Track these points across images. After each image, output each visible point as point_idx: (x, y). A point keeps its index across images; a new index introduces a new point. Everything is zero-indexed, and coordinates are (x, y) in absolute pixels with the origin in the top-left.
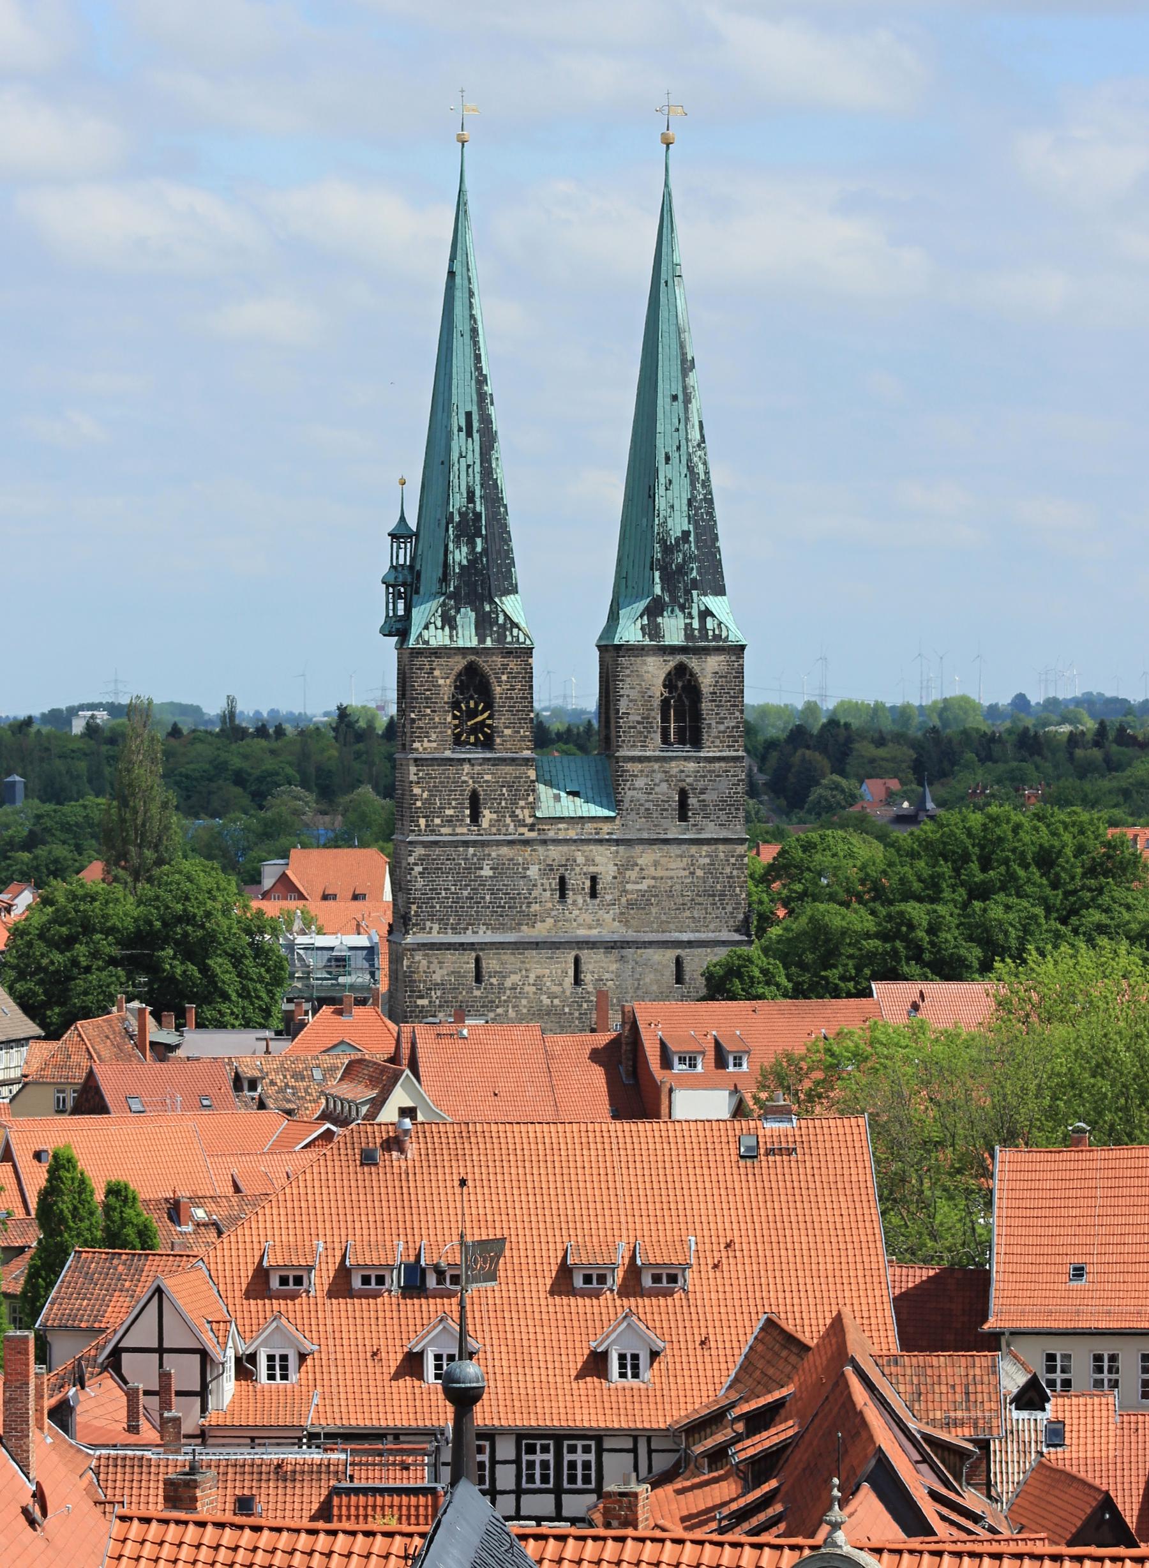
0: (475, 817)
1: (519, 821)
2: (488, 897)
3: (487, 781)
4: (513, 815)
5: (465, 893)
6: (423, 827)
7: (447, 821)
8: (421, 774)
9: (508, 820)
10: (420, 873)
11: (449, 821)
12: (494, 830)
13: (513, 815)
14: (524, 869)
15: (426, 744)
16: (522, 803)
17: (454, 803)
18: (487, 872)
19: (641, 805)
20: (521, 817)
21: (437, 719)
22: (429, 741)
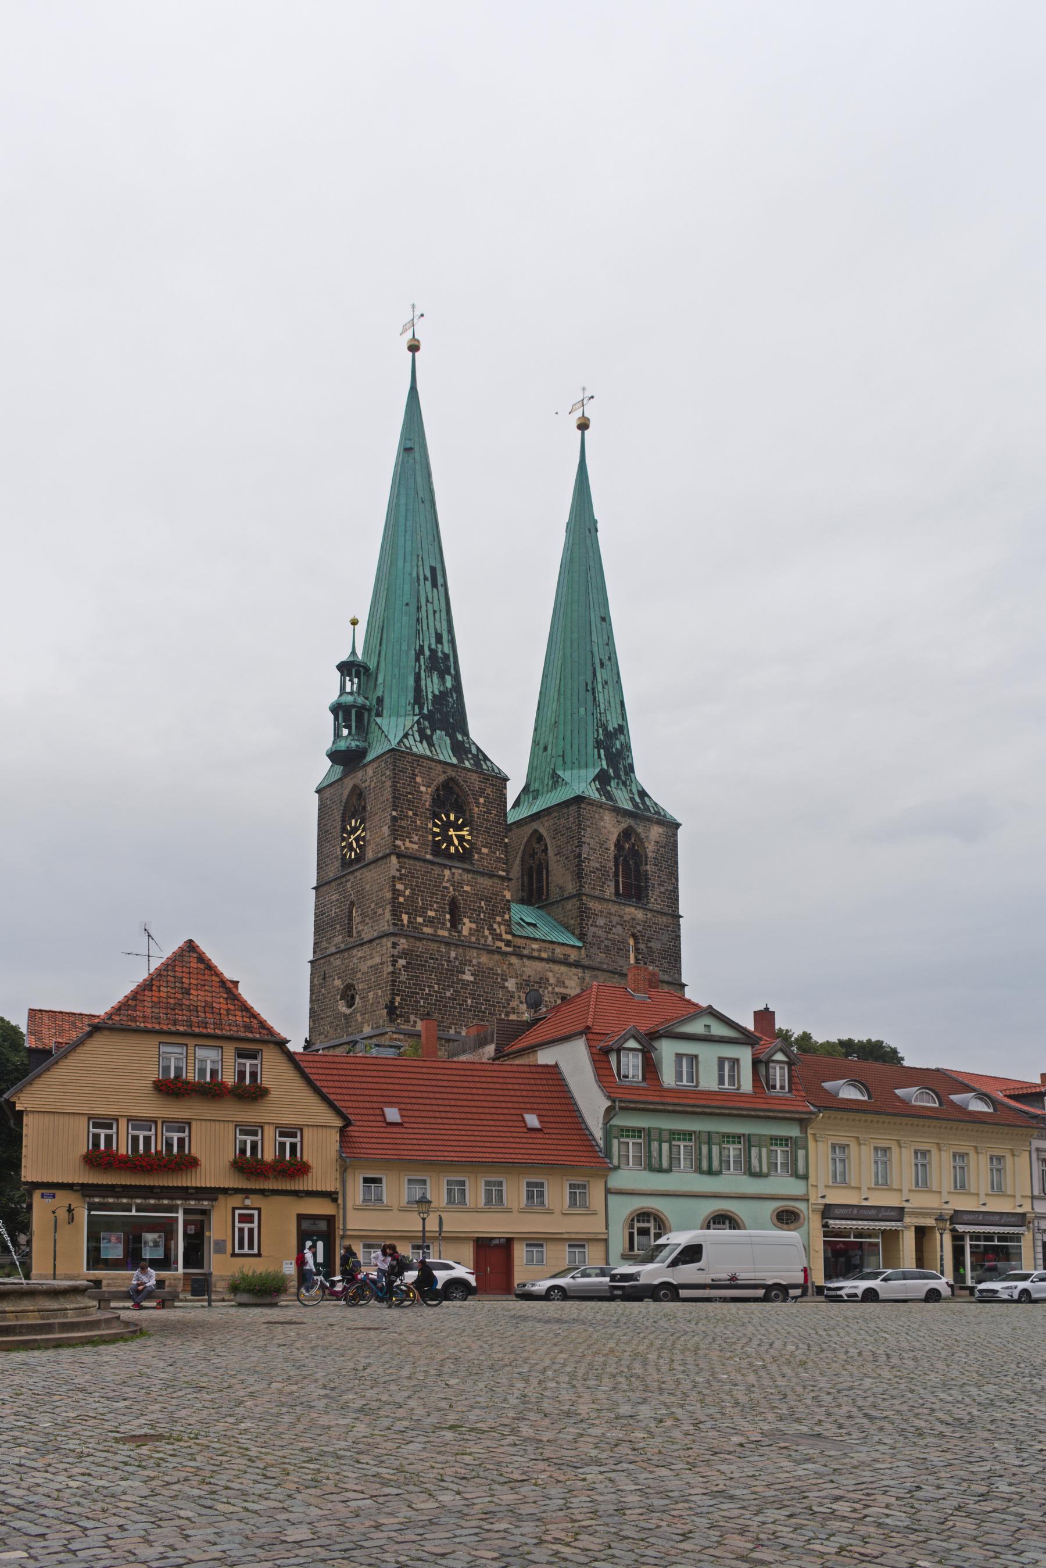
0: (455, 922)
1: (497, 935)
2: (469, 1001)
4: (491, 929)
5: (448, 994)
6: (405, 922)
7: (429, 921)
8: (403, 871)
9: (487, 932)
10: (403, 966)
11: (430, 921)
12: (473, 939)
13: (491, 929)
14: (502, 979)
15: (408, 844)
16: (499, 919)
19: (602, 941)
21: (419, 823)
22: (411, 842)
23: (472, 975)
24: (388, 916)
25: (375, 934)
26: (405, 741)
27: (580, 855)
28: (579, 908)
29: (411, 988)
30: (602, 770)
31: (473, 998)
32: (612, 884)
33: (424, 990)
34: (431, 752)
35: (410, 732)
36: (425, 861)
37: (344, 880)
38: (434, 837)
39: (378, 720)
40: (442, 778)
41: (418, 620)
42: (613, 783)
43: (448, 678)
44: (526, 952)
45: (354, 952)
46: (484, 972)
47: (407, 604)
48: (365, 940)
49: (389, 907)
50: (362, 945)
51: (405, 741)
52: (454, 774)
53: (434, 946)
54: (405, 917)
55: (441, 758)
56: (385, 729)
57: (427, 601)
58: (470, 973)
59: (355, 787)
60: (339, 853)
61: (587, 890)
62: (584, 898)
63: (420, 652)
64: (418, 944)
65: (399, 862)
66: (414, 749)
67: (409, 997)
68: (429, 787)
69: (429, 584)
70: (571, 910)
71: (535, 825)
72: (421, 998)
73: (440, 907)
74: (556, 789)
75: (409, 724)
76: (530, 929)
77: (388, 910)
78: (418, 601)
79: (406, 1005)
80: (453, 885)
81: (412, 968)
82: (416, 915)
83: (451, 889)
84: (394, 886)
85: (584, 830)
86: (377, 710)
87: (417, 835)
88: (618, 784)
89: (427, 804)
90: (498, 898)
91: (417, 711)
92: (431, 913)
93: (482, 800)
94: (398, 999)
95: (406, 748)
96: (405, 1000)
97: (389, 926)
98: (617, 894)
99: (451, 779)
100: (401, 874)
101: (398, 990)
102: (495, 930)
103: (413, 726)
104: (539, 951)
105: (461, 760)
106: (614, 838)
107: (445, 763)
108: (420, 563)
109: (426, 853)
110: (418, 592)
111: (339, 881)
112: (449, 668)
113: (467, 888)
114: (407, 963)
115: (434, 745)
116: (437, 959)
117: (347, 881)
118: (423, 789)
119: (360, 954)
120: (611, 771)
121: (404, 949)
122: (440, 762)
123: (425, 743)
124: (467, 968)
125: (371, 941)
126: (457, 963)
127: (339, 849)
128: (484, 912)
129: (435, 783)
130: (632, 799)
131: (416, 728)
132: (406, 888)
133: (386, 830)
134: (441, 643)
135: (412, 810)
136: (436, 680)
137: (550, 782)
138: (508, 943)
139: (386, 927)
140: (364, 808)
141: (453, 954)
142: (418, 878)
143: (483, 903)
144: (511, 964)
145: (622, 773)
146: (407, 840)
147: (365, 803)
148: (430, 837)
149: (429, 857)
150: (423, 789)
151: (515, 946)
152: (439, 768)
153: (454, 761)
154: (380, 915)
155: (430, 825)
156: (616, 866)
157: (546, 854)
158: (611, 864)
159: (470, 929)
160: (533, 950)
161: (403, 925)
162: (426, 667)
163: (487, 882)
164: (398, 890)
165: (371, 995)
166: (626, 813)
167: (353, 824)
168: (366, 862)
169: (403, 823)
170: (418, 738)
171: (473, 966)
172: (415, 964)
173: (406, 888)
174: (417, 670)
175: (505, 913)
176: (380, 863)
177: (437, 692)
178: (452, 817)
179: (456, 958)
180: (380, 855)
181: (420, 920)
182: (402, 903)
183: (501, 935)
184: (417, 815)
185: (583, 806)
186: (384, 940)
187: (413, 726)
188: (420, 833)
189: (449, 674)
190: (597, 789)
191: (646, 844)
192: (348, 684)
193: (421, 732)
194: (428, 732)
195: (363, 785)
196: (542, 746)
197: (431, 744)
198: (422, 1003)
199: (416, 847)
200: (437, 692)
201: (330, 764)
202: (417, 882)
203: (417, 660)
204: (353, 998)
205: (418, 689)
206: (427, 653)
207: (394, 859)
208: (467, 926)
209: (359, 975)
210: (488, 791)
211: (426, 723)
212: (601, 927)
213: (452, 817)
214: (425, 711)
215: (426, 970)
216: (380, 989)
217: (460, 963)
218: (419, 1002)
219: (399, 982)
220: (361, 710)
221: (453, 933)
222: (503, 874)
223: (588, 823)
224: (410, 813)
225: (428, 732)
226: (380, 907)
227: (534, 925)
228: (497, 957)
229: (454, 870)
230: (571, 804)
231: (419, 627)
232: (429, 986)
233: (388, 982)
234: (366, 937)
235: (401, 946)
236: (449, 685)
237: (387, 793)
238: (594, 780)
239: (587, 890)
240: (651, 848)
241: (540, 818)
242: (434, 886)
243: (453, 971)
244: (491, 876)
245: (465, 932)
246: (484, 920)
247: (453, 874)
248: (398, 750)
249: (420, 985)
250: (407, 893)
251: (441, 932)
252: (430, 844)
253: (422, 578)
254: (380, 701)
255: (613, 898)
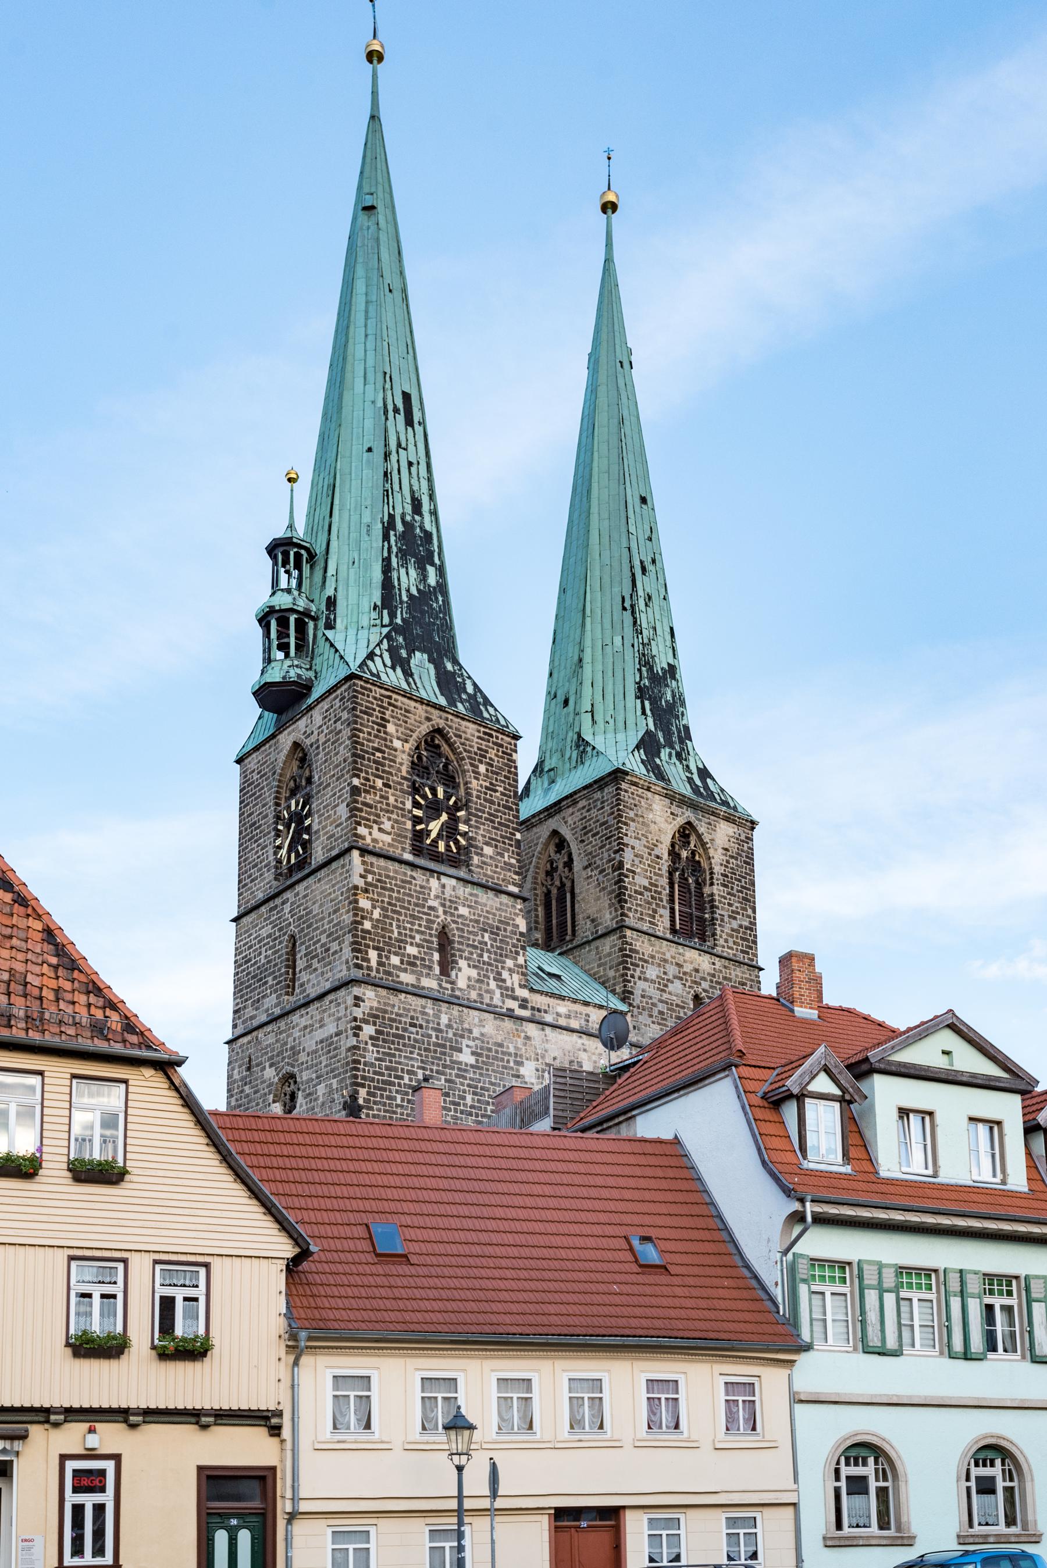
0: (447, 966)
1: (507, 989)
3: (459, 916)
4: (499, 978)
6: (374, 963)
7: (411, 964)
8: (370, 878)
9: (493, 984)
10: (371, 1038)
11: (411, 963)
13: (499, 978)
15: (376, 834)
16: (509, 963)
17: (418, 937)
18: (466, 1057)
20: (509, 984)
21: (392, 800)
22: (380, 830)
23: (473, 1053)
24: (347, 952)
25: (328, 986)
26: (369, 663)
27: (621, 865)
28: (621, 950)
29: (383, 1075)
30: (648, 732)
31: (475, 1093)
32: (666, 913)
33: (402, 1078)
34: (409, 684)
35: (377, 651)
36: (402, 862)
37: (278, 901)
38: (414, 826)
39: (329, 634)
40: (425, 728)
41: (386, 474)
42: (664, 753)
43: (431, 571)
44: (549, 1018)
45: (295, 1018)
46: (490, 1050)
47: (370, 450)
48: (313, 996)
49: (349, 939)
50: (306, 1004)
51: (369, 663)
52: (442, 723)
53: (416, 1003)
54: (373, 955)
55: (424, 695)
56: (339, 646)
57: (399, 445)
58: (469, 1050)
59: (296, 745)
60: (271, 858)
61: (630, 921)
62: (628, 933)
63: (389, 526)
64: (393, 999)
65: (364, 863)
66: (383, 677)
67: (380, 1089)
68: (406, 741)
69: (401, 418)
70: (610, 954)
71: (553, 824)
72: (397, 1092)
73: (425, 940)
74: (582, 763)
75: (375, 639)
76: (553, 982)
77: (347, 943)
78: (386, 445)
79: (375, 1103)
80: (443, 905)
81: (384, 1041)
82: (389, 952)
83: (441, 910)
84: (356, 901)
85: (626, 824)
86: (327, 618)
87: (389, 819)
88: (670, 755)
89: (404, 769)
90: (509, 928)
91: (386, 620)
92: (411, 950)
93: (482, 768)
94: (363, 1093)
95: (372, 674)
96: (374, 1095)
97: (348, 969)
98: (673, 931)
99: (439, 731)
100: (366, 883)
101: (364, 1078)
102: (504, 981)
103: (381, 642)
104: (568, 1017)
105: (452, 703)
106: (667, 840)
107: (429, 704)
108: (388, 386)
109: (403, 849)
110: (386, 431)
111: (271, 904)
112: (432, 553)
113: (463, 911)
114: (377, 1032)
115: (412, 675)
116: (421, 1027)
117: (283, 903)
118: (397, 744)
119: (304, 1022)
120: (660, 735)
121: (371, 1008)
122: (421, 701)
123: (399, 670)
124: (465, 1042)
125: (321, 997)
126: (450, 1035)
127: (271, 852)
128: (488, 951)
129: (415, 736)
130: (690, 780)
131: (385, 645)
132: (374, 907)
133: (343, 811)
134: (420, 514)
135: (382, 778)
136: (413, 573)
137: (575, 754)
138: (524, 1004)
139: (344, 972)
140: (309, 780)
141: (444, 1019)
142: (392, 890)
143: (486, 935)
144: (528, 1038)
145: (675, 739)
146: (375, 826)
147: (311, 771)
148: (409, 825)
149: (408, 856)
150: (397, 744)
151: (533, 1008)
152: (421, 710)
153: (442, 701)
154: (336, 952)
155: (409, 805)
156: (671, 884)
157: (571, 870)
158: (664, 881)
159: (469, 979)
160: (558, 1014)
161: (369, 968)
162: (400, 550)
163: (488, 899)
164: (363, 910)
165: (321, 1089)
166: (683, 801)
167: (293, 808)
168: (313, 866)
169: (369, 799)
170: (389, 663)
171: (474, 1039)
172: (388, 1034)
173: (374, 907)
174: (386, 554)
175: (517, 953)
176: (334, 865)
177: (414, 591)
178: (440, 792)
179: (449, 1026)
180: (334, 853)
181: (395, 960)
182: (368, 932)
183: (513, 990)
184: (389, 787)
185: (624, 786)
186: (342, 993)
187: (381, 642)
188: (394, 816)
189: (433, 564)
190: (643, 761)
191: (711, 852)
192: (283, 578)
193: (393, 651)
194: (404, 653)
195: (308, 742)
196: (561, 698)
197: (408, 673)
198: (399, 1101)
199: (388, 839)
200: (414, 591)
201: (259, 710)
202: (390, 897)
203: (386, 537)
204: (293, 1097)
205: (387, 585)
206: (400, 527)
207: (355, 853)
208: (464, 974)
209: (303, 1057)
210: (492, 753)
211: (401, 639)
212: (653, 982)
213: (440, 792)
214: (399, 621)
215: (404, 1045)
216: (334, 1077)
217: (455, 1035)
218: (395, 1099)
219: (365, 1064)
220: (304, 617)
221: (444, 985)
222: (515, 890)
223: (632, 814)
224: (379, 783)
225: (404, 653)
226: (334, 940)
227: (558, 977)
228: (508, 1024)
229: (444, 880)
230: (606, 785)
231: (388, 486)
232: (409, 1072)
233: (347, 1064)
234: (313, 992)
235: (367, 1004)
236: (432, 580)
237: (344, 752)
238: (638, 747)
239: (630, 921)
240: (718, 857)
241: (560, 811)
242: (416, 905)
243: (444, 1046)
244: (499, 891)
245: (462, 983)
246: (490, 964)
247: (444, 886)
248: (360, 678)
249: (396, 1069)
250: (376, 914)
251: (426, 982)
252: (410, 835)
253: (390, 408)
254: (331, 603)
255: (669, 936)
